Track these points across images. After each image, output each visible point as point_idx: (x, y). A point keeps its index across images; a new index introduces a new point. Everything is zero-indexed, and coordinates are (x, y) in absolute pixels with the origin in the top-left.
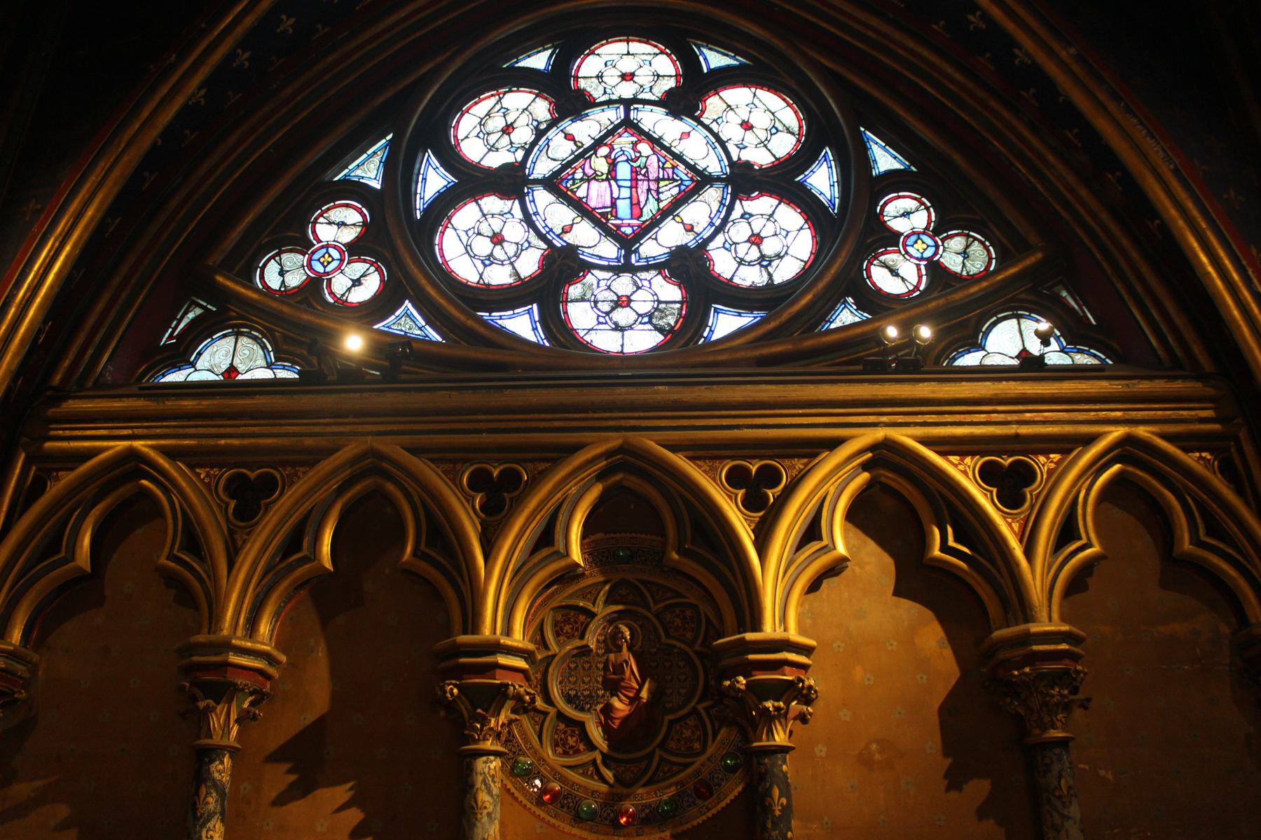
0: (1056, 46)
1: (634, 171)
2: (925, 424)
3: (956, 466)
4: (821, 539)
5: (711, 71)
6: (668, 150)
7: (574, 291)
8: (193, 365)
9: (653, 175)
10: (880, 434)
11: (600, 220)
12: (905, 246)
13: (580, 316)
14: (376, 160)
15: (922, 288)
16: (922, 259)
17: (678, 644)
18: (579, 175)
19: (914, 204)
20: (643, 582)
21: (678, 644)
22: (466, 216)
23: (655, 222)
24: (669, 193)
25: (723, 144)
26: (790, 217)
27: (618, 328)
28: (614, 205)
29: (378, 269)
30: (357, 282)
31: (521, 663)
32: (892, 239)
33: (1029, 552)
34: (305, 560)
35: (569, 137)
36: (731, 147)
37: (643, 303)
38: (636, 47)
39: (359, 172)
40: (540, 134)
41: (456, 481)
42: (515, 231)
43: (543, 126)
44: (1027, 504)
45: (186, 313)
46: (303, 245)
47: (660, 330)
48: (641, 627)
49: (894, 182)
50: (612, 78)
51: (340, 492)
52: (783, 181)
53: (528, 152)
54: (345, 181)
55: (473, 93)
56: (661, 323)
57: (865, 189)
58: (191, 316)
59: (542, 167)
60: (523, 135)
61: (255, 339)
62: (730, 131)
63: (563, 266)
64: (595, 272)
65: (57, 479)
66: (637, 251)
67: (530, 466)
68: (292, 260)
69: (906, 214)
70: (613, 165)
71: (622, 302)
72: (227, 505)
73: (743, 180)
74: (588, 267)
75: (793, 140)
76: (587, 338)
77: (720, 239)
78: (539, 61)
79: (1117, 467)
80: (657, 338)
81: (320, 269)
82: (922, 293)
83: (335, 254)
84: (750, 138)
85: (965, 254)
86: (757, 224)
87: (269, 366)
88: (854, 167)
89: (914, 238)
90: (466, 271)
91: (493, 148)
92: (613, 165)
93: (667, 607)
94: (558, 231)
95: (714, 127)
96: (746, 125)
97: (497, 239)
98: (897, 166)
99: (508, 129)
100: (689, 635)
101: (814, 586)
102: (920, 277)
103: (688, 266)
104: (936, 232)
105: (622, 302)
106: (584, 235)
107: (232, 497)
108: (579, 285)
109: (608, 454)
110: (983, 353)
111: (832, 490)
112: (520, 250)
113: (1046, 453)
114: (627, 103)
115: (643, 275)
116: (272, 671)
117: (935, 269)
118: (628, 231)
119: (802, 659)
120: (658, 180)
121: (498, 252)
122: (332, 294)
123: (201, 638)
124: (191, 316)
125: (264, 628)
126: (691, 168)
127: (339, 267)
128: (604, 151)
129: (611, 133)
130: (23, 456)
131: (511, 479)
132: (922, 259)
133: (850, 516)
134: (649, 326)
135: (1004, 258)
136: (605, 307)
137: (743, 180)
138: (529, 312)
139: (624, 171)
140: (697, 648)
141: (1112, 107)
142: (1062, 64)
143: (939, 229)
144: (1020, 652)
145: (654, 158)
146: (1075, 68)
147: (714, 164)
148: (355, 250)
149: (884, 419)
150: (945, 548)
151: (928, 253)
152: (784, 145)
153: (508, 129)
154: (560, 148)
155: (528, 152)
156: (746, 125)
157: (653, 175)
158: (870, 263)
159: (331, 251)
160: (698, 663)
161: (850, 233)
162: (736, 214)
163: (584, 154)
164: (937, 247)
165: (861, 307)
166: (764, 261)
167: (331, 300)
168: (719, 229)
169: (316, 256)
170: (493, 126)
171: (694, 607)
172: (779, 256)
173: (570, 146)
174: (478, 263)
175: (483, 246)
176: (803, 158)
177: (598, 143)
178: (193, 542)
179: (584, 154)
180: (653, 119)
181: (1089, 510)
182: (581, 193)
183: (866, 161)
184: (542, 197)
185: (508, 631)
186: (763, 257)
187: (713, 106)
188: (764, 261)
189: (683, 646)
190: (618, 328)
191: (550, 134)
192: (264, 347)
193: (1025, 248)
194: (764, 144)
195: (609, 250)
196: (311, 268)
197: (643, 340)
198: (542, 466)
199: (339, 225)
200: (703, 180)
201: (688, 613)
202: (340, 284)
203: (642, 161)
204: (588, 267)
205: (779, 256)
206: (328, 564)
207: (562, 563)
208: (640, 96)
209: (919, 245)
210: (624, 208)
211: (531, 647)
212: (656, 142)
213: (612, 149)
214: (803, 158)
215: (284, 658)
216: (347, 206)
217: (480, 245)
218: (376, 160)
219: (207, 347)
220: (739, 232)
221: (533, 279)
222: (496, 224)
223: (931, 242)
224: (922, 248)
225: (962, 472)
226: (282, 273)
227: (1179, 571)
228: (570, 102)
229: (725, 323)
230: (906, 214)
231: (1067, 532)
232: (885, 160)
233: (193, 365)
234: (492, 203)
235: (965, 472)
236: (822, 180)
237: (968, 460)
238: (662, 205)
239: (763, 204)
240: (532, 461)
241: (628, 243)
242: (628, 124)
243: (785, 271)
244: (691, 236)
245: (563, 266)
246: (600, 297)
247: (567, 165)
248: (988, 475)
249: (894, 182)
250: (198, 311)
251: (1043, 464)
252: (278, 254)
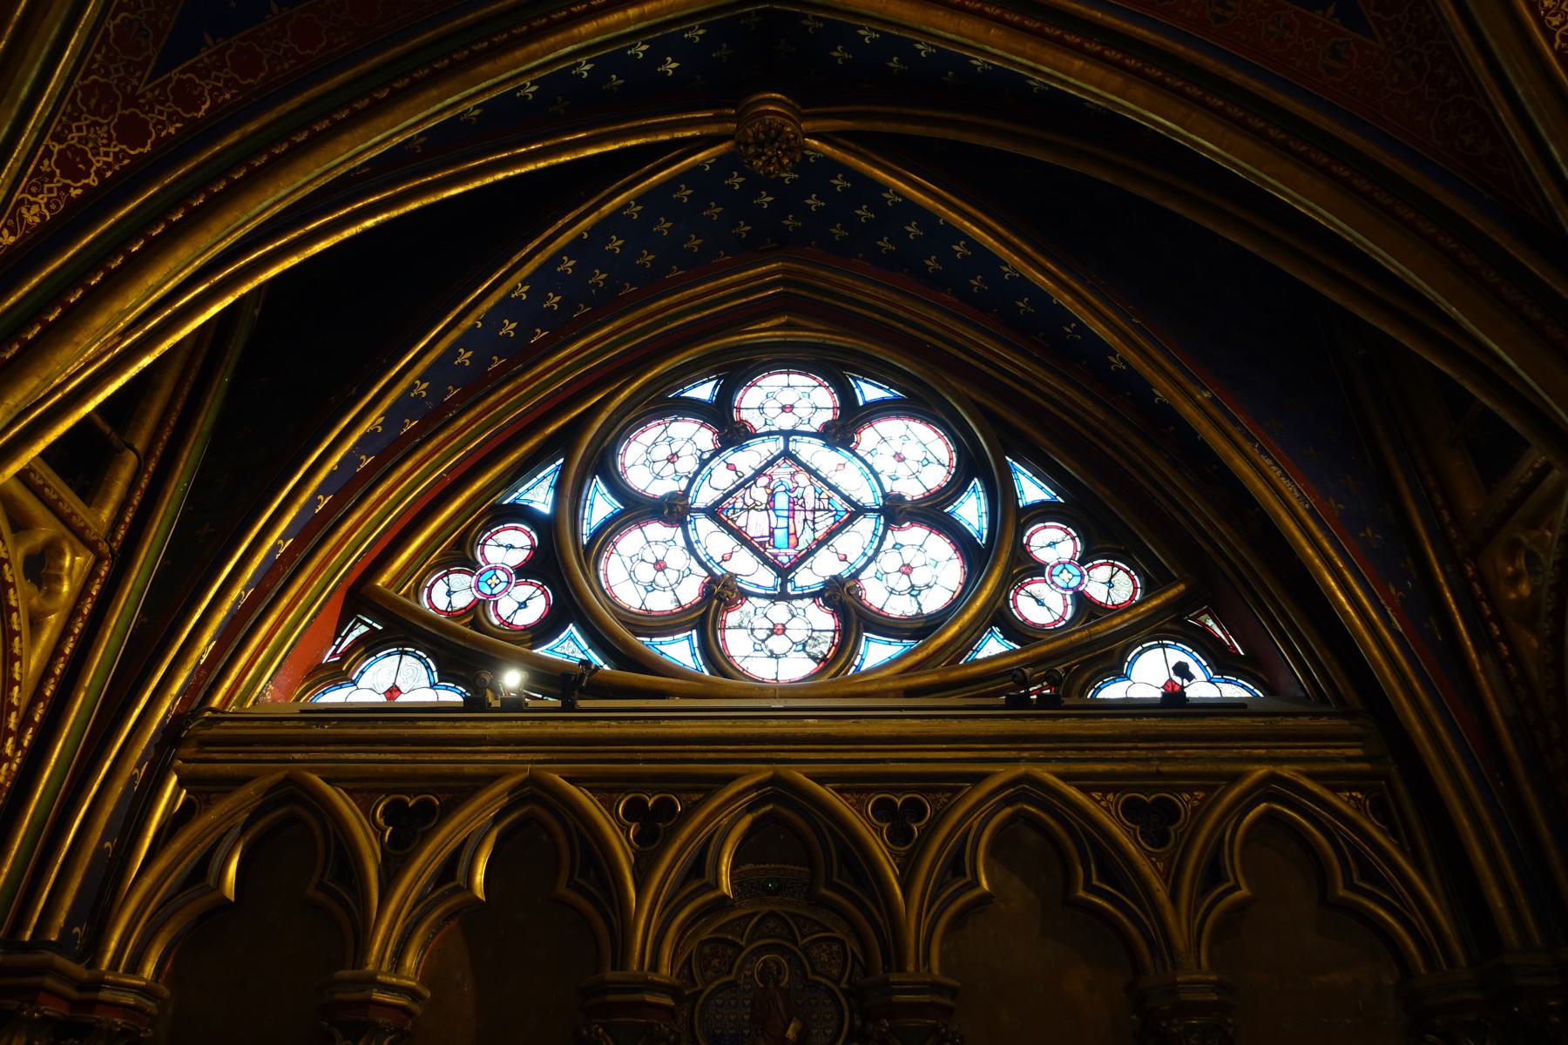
0: (1193, 389)
1: (792, 502)
2: (1066, 760)
3: (1098, 802)
4: (965, 875)
5: (866, 403)
6: (824, 481)
7: (732, 618)
8: (354, 683)
9: (809, 506)
10: (1022, 769)
11: (756, 548)
12: (1051, 575)
13: (736, 643)
14: (546, 484)
15: (1068, 617)
16: (1068, 589)
17: (824, 981)
18: (739, 505)
19: (1062, 534)
20: (793, 915)
21: (824, 981)
22: (631, 542)
23: (810, 552)
24: (825, 523)
25: (876, 475)
26: (940, 547)
27: (772, 655)
28: (772, 535)
29: (544, 592)
30: (523, 605)
31: (667, 1001)
32: (1037, 569)
33: (1174, 897)
34: (458, 889)
35: (731, 467)
36: (883, 478)
37: (798, 631)
38: (796, 379)
39: (527, 496)
40: (703, 463)
41: (611, 809)
42: (678, 558)
43: (706, 456)
44: (1171, 844)
45: (351, 630)
46: (470, 565)
47: (814, 658)
48: (789, 962)
49: (1041, 512)
50: (772, 410)
51: (496, 820)
52: (932, 513)
53: (692, 481)
54: (513, 505)
55: (641, 421)
56: (815, 651)
57: (1011, 518)
58: (356, 633)
59: (704, 496)
60: (688, 464)
61: (420, 658)
62: (884, 463)
63: (721, 594)
64: (753, 599)
67: (685, 796)
68: (460, 581)
69: (1052, 543)
70: (772, 496)
71: (777, 630)
72: (384, 832)
73: (894, 511)
74: (745, 595)
75: (944, 471)
76: (744, 665)
77: (872, 567)
78: (704, 391)
79: (1263, 805)
80: (812, 666)
81: (488, 591)
82: (1069, 623)
83: (503, 576)
84: (902, 469)
85: (1110, 584)
86: (909, 555)
87: (433, 686)
88: (1001, 496)
89: (1060, 567)
90: (629, 596)
91: (658, 476)
92: (772, 496)
93: (813, 942)
94: (718, 559)
95: (869, 459)
96: (899, 458)
97: (660, 566)
98: (1046, 497)
99: (672, 458)
100: (835, 972)
101: (958, 922)
102: (1066, 607)
103: (838, 593)
104: (1082, 562)
105: (777, 630)
106: (744, 566)
107: (388, 823)
108: (736, 613)
109: (758, 786)
110: (1128, 683)
111: (976, 824)
112: (683, 575)
113: (1190, 790)
114: (787, 434)
115: (797, 603)
116: (415, 1008)
117: (1081, 600)
118: (785, 560)
119: (946, 1001)
120: (814, 511)
121: (661, 579)
122: (497, 615)
123: (346, 973)
124: (356, 633)
125: (410, 961)
126: (846, 499)
127: (505, 590)
128: (763, 481)
129: (770, 463)
130: (174, 779)
131: (665, 807)
132: (1068, 589)
133: (992, 851)
134: (803, 654)
135: (1150, 588)
136: (762, 634)
137: (894, 511)
138: (689, 638)
139: (782, 501)
140: (844, 985)
141: (1247, 447)
142: (1198, 405)
143: (1086, 558)
145: (810, 490)
146: (1213, 411)
147: (867, 495)
148: (523, 572)
149: (1026, 754)
151: (1074, 583)
152: (936, 477)
153: (672, 458)
154: (722, 478)
155: (692, 481)
156: (899, 458)
157: (809, 506)
158: (1017, 593)
159: (499, 573)
160: (843, 1000)
161: (998, 560)
162: (888, 544)
163: (745, 484)
164: (1082, 576)
165: (1007, 637)
166: (914, 591)
167: (496, 622)
168: (871, 560)
169: (483, 578)
170: (658, 455)
171: (841, 942)
172: (928, 586)
173: (732, 476)
174: (641, 589)
175: (646, 573)
176: (955, 488)
177: (759, 473)
179: (745, 484)
180: (812, 451)
181: (1236, 850)
182: (741, 522)
183: (1010, 492)
184: (704, 527)
185: (655, 966)
186: (913, 587)
187: (868, 437)
188: (914, 591)
189: (829, 984)
190: (772, 655)
191: (713, 463)
192: (428, 667)
193: (1169, 581)
194: (915, 475)
195: (767, 578)
196: (477, 587)
197: (797, 668)
198: (697, 797)
199: (508, 547)
200: (857, 511)
201: (835, 948)
202: (506, 607)
203: (798, 492)
204: (745, 595)
205: (928, 586)
206: (480, 894)
207: (712, 895)
208: (800, 428)
209: (1065, 575)
210: (780, 535)
211: (677, 982)
212: (812, 473)
213: (771, 479)
214: (955, 488)
215: (428, 994)
216: (516, 529)
217: (643, 573)
218: (546, 484)
219: (370, 665)
220: (889, 561)
221: (694, 607)
222: (659, 552)
223: (1076, 572)
224: (1068, 578)
225: (1103, 812)
226: (449, 593)
228: (733, 434)
229: (876, 652)
230: (1052, 544)
231: (1213, 873)
232: (1031, 490)
233: (354, 683)
234: (656, 530)
235: (1107, 809)
236: (972, 511)
237: (1110, 797)
238: (818, 535)
239: (914, 534)
240: (686, 791)
241: (784, 572)
242: (787, 454)
243: (934, 602)
244: (845, 565)
245: (721, 594)
246: (756, 625)
247: (729, 494)
248: (1132, 810)
249: (1041, 512)
250: (364, 629)
251: (1185, 801)
252: (446, 575)
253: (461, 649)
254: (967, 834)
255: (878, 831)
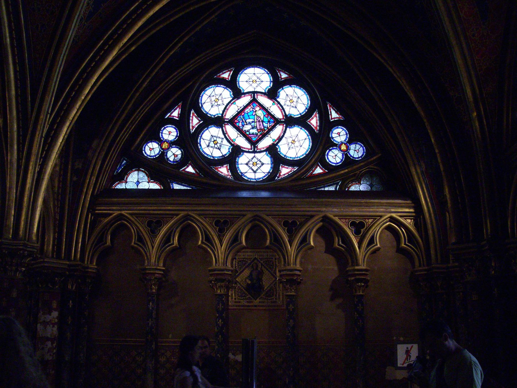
13: (242, 168)
49: (337, 123)
57: (327, 126)
63: (237, 151)
65: (101, 221)
66: (257, 147)
69: (339, 135)
78: (226, 75)
88: (324, 118)
138: (226, 167)
144: (352, 273)
150: (339, 245)
161: (321, 141)
178: (140, 239)
180: (264, 100)
227: (400, 250)
232: (334, 115)
253: (157, 168)
254: (308, 231)
255: (284, 230)
